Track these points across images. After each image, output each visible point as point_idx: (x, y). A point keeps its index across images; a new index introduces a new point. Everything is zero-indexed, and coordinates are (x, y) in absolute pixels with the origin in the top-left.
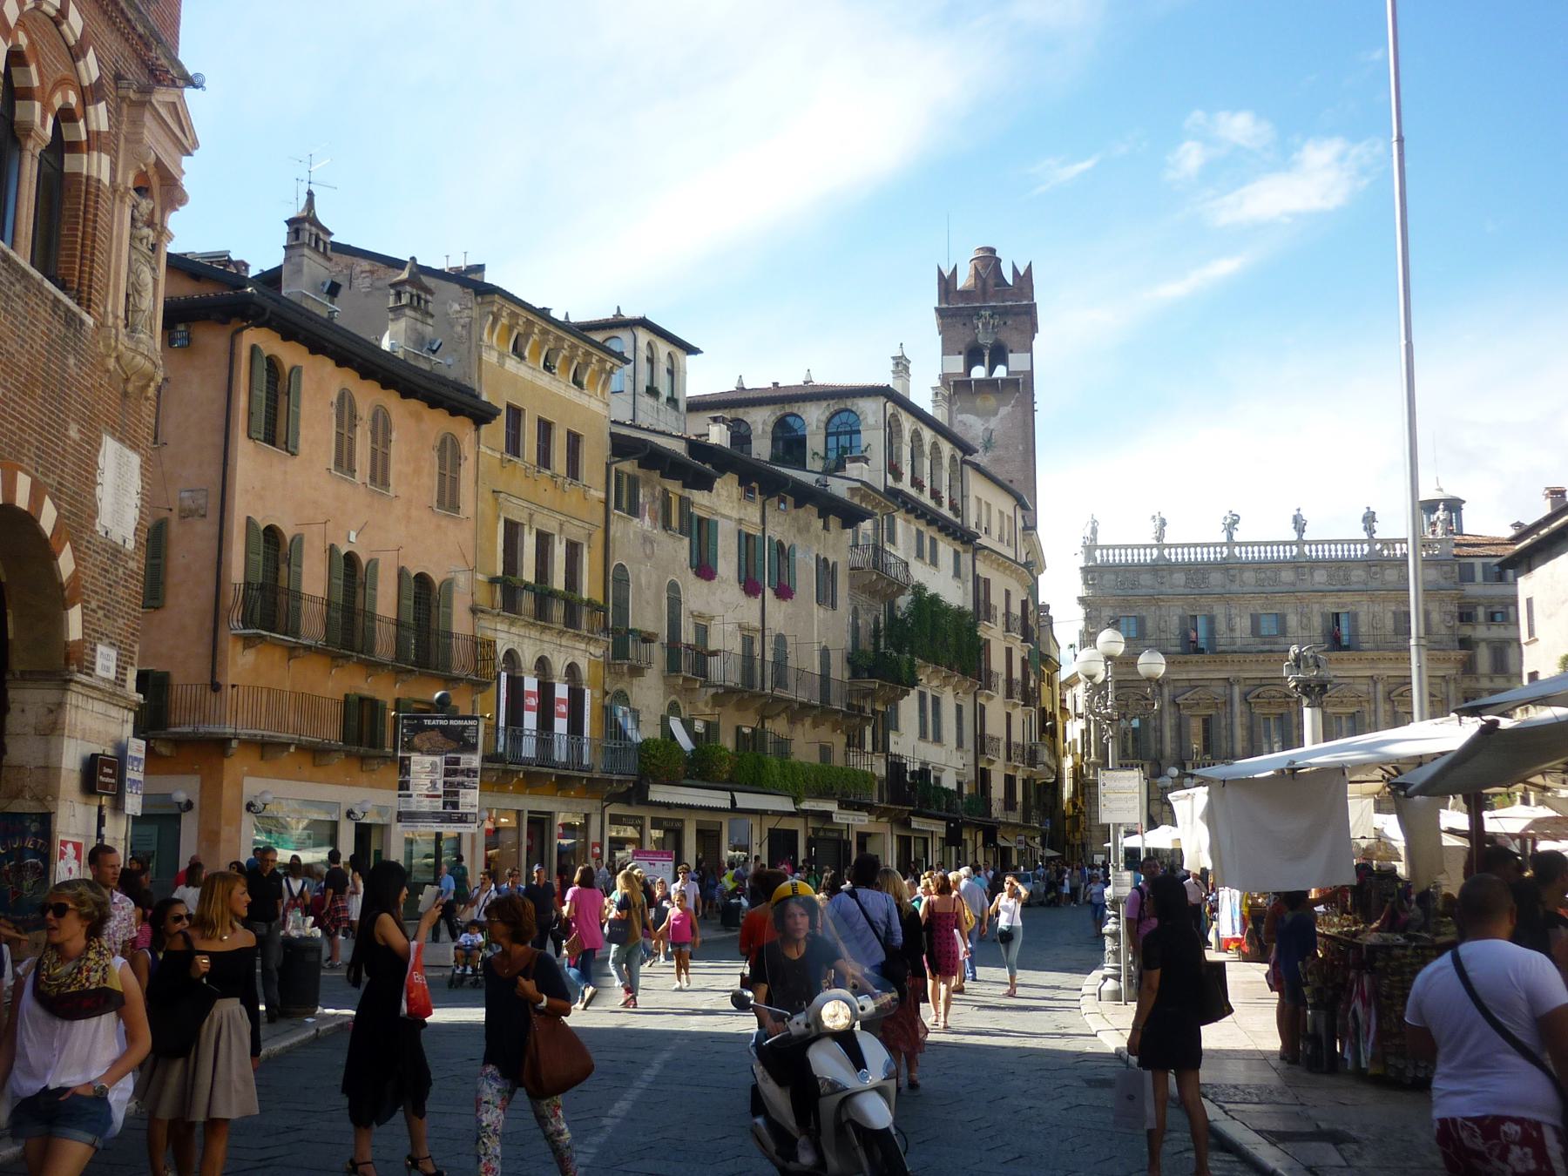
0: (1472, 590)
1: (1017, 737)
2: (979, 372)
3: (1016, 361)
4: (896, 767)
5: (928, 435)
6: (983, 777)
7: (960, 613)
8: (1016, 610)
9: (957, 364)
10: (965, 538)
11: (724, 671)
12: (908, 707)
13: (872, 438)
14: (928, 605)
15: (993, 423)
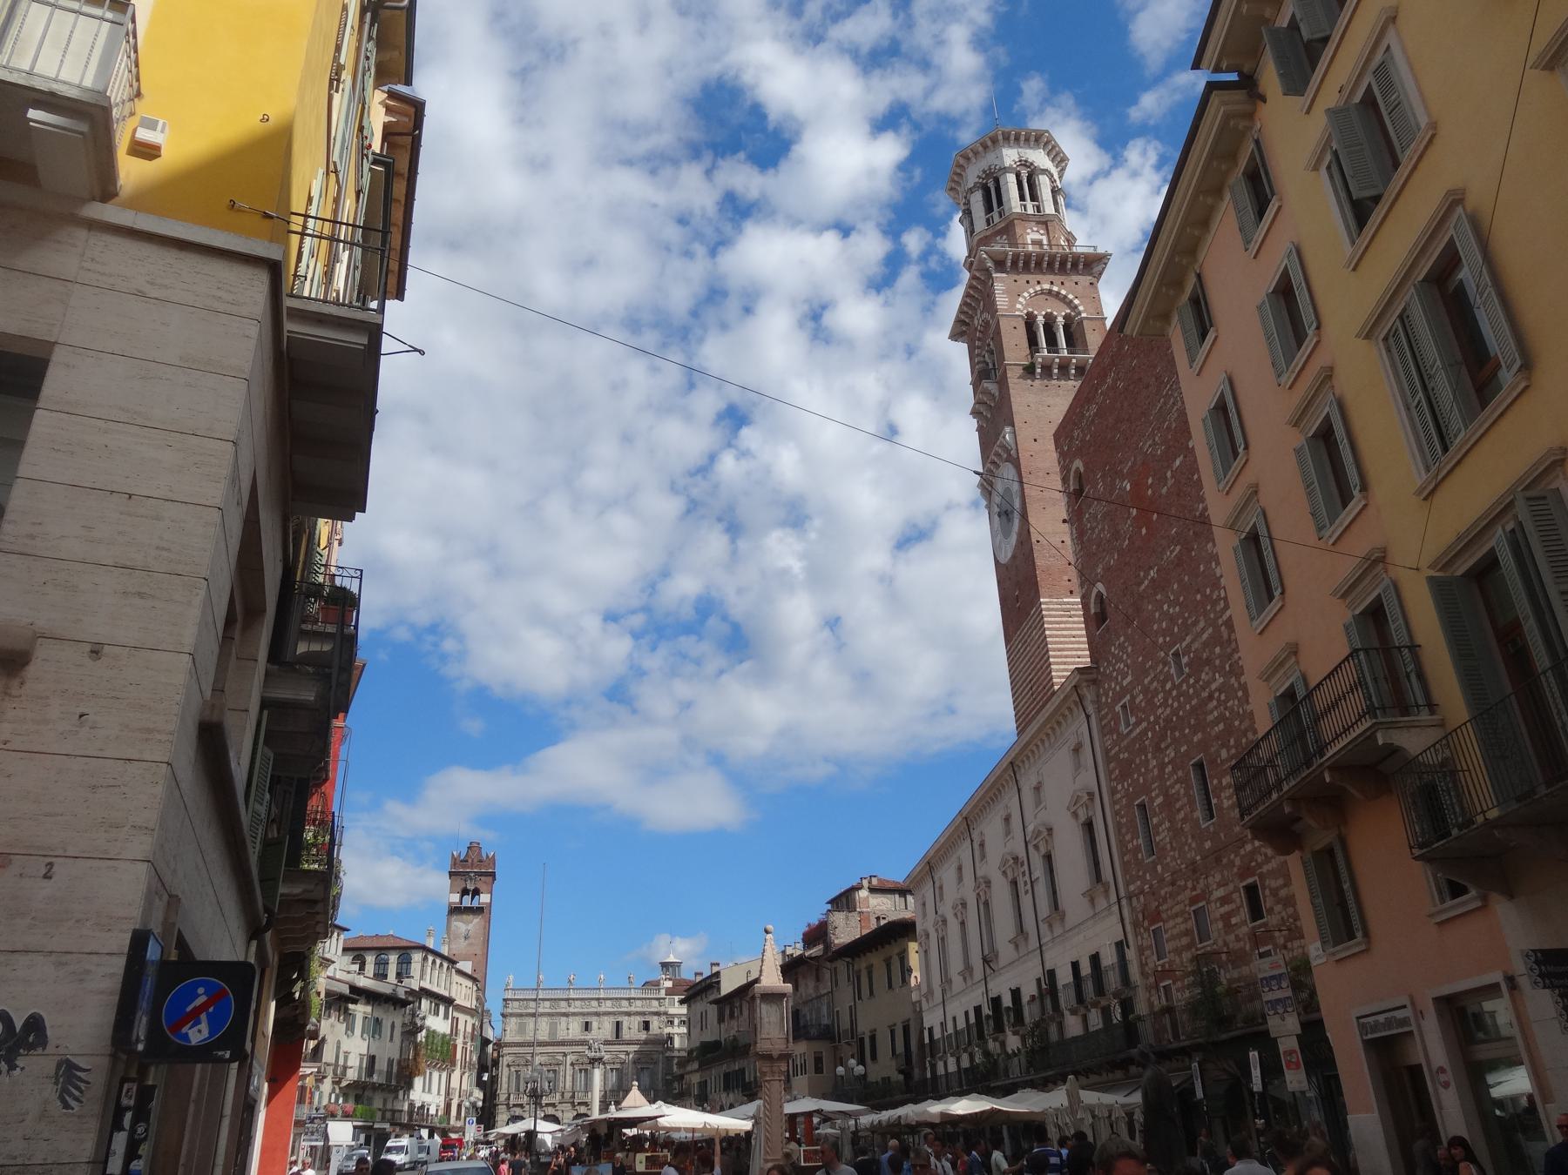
0: (672, 1011)
1: (464, 1087)
2: (467, 901)
3: (484, 898)
4: (412, 1105)
5: (438, 961)
6: (448, 1106)
7: (444, 1035)
8: (469, 1029)
9: (455, 898)
10: (448, 1001)
11: (352, 1075)
12: (418, 1082)
13: (415, 967)
14: (432, 1034)
15: (470, 927)
